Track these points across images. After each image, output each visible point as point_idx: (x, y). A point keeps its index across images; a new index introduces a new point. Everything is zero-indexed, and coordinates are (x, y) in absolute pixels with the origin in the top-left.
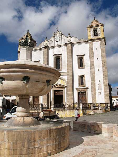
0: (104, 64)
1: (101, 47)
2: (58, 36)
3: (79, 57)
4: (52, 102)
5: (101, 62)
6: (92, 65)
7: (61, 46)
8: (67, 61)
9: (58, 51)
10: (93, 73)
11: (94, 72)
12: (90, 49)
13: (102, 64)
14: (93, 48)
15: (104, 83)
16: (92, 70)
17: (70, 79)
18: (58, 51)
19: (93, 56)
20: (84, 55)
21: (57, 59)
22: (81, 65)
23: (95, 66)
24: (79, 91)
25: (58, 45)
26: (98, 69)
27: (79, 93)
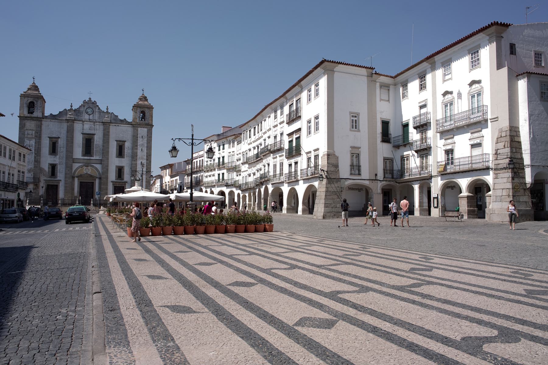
0: (148, 157)
1: (147, 136)
2: (91, 106)
3: (119, 142)
4: (77, 196)
5: (145, 154)
6: (134, 157)
7: (94, 122)
8: (103, 146)
9: (90, 129)
10: (134, 166)
11: (136, 164)
12: (134, 136)
13: (147, 156)
14: (139, 136)
15: (146, 178)
16: (134, 162)
17: (105, 169)
18: (90, 129)
19: (137, 146)
20: (126, 141)
21: (86, 139)
22: (120, 153)
23: (138, 158)
24: (115, 185)
25: (89, 119)
26: (141, 162)
27: (115, 186)
